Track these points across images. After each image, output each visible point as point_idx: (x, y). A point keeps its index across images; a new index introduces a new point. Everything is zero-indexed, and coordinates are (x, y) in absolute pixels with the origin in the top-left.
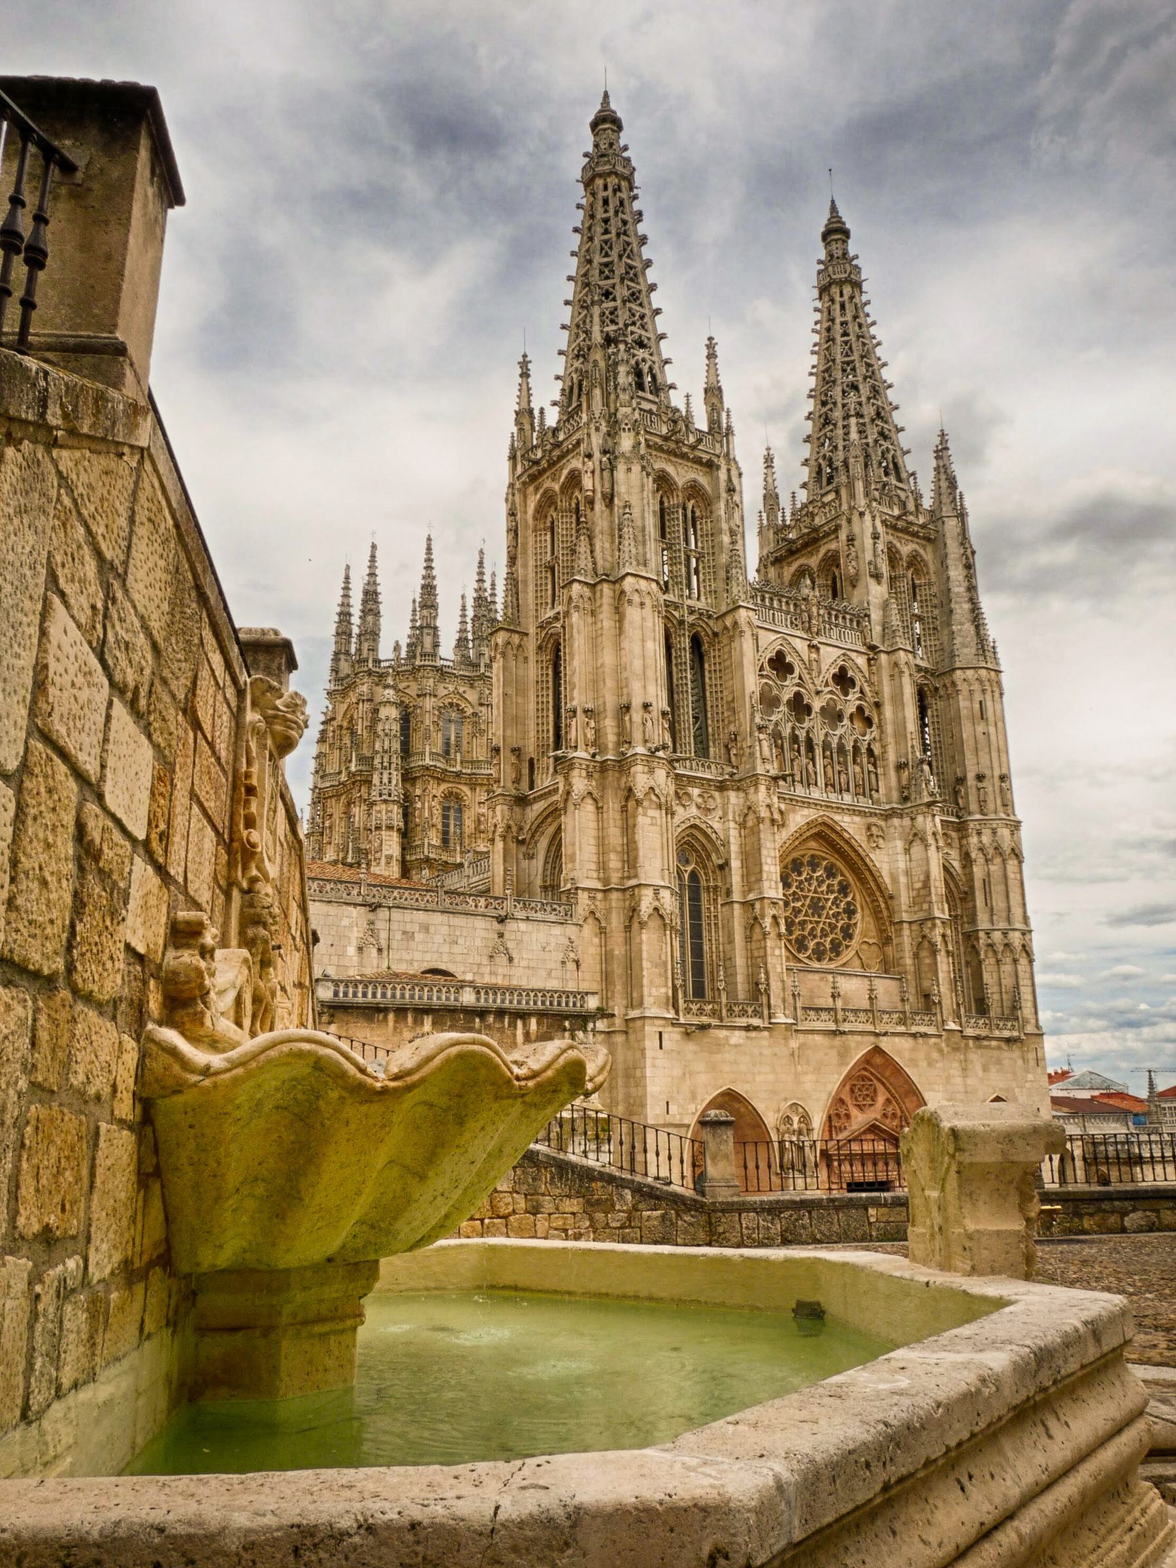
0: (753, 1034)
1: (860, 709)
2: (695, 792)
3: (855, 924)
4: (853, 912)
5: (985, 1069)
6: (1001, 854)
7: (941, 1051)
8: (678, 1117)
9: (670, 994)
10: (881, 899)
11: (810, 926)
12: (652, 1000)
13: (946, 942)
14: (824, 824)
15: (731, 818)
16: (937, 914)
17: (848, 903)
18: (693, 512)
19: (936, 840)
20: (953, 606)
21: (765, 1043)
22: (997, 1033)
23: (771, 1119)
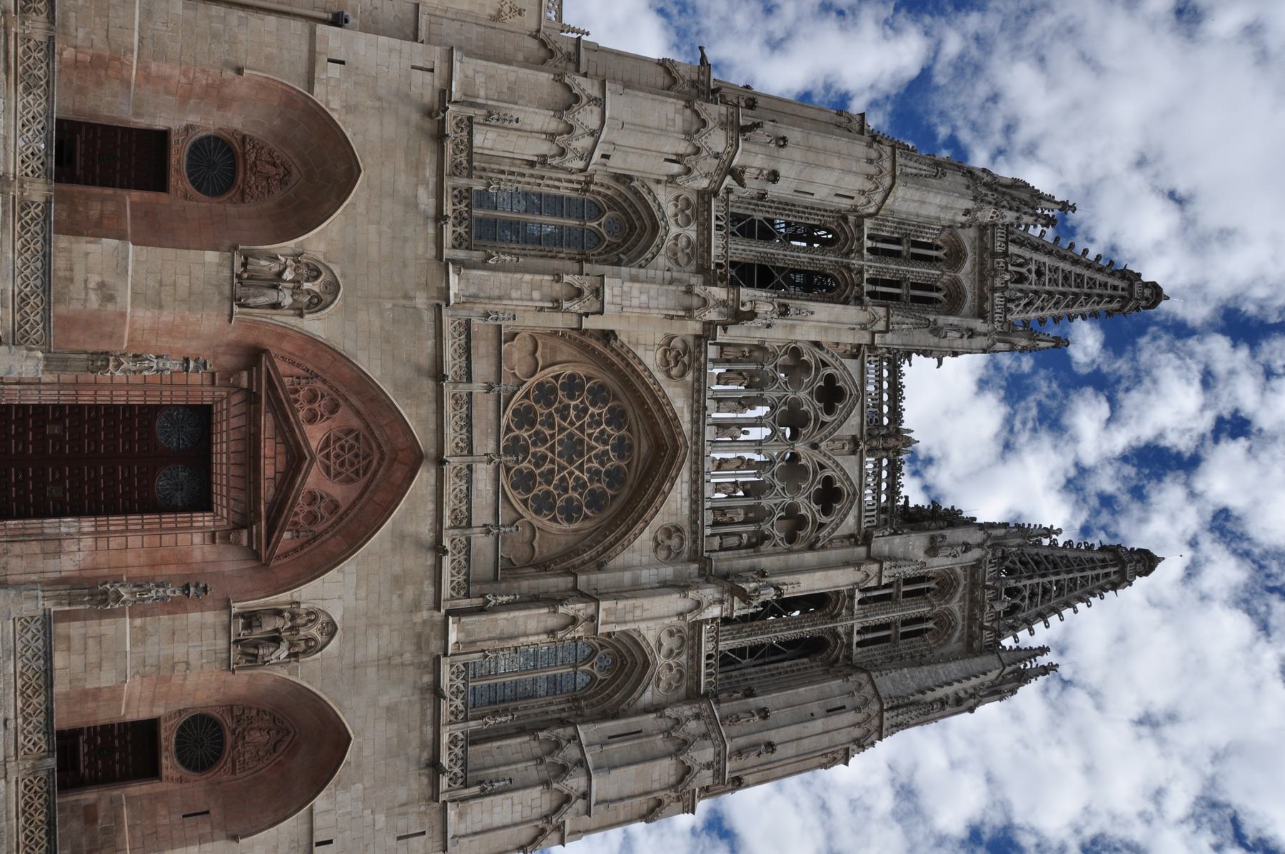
0: (431, 230)
1: (801, 522)
2: (691, 232)
3: (554, 519)
4: (570, 520)
5: (391, 711)
6: (679, 750)
7: (416, 606)
8: (323, 76)
9: (479, 101)
10: (592, 553)
11: (548, 432)
12: (470, 73)
13: (564, 628)
14: (676, 449)
15: (676, 275)
16: (603, 605)
17: (579, 509)
18: (937, 301)
19: (690, 611)
20: (925, 668)
21: (420, 250)
22: (445, 739)
23: (315, 242)
